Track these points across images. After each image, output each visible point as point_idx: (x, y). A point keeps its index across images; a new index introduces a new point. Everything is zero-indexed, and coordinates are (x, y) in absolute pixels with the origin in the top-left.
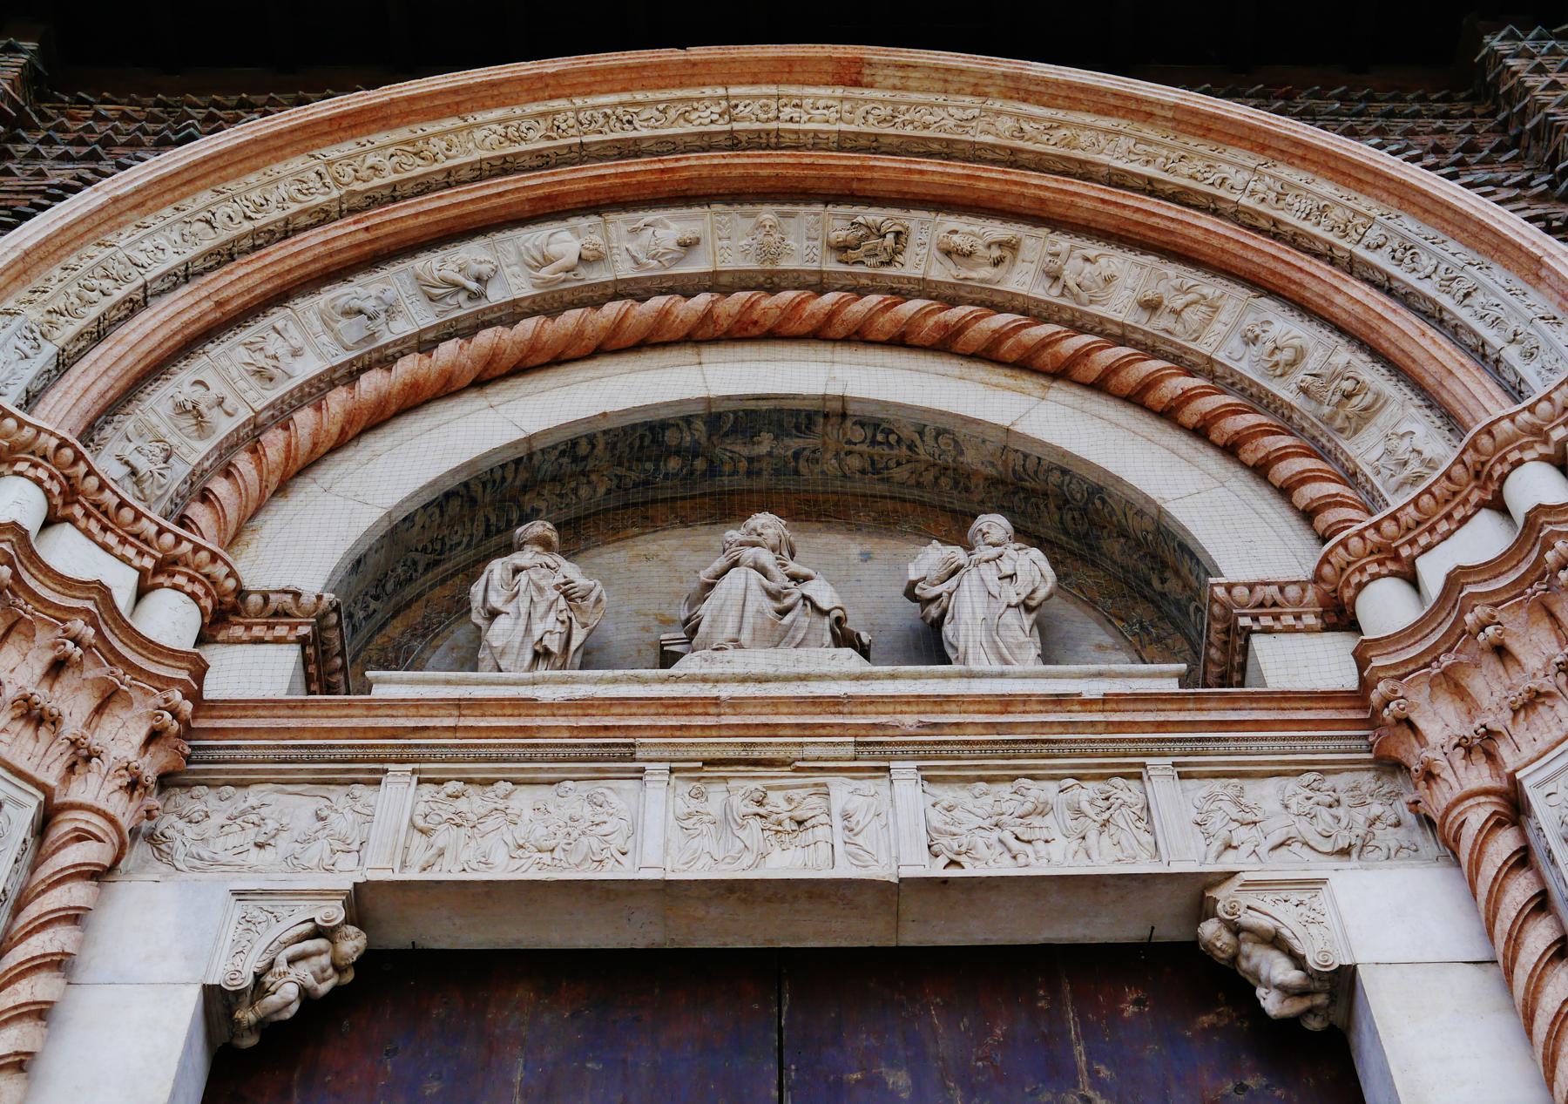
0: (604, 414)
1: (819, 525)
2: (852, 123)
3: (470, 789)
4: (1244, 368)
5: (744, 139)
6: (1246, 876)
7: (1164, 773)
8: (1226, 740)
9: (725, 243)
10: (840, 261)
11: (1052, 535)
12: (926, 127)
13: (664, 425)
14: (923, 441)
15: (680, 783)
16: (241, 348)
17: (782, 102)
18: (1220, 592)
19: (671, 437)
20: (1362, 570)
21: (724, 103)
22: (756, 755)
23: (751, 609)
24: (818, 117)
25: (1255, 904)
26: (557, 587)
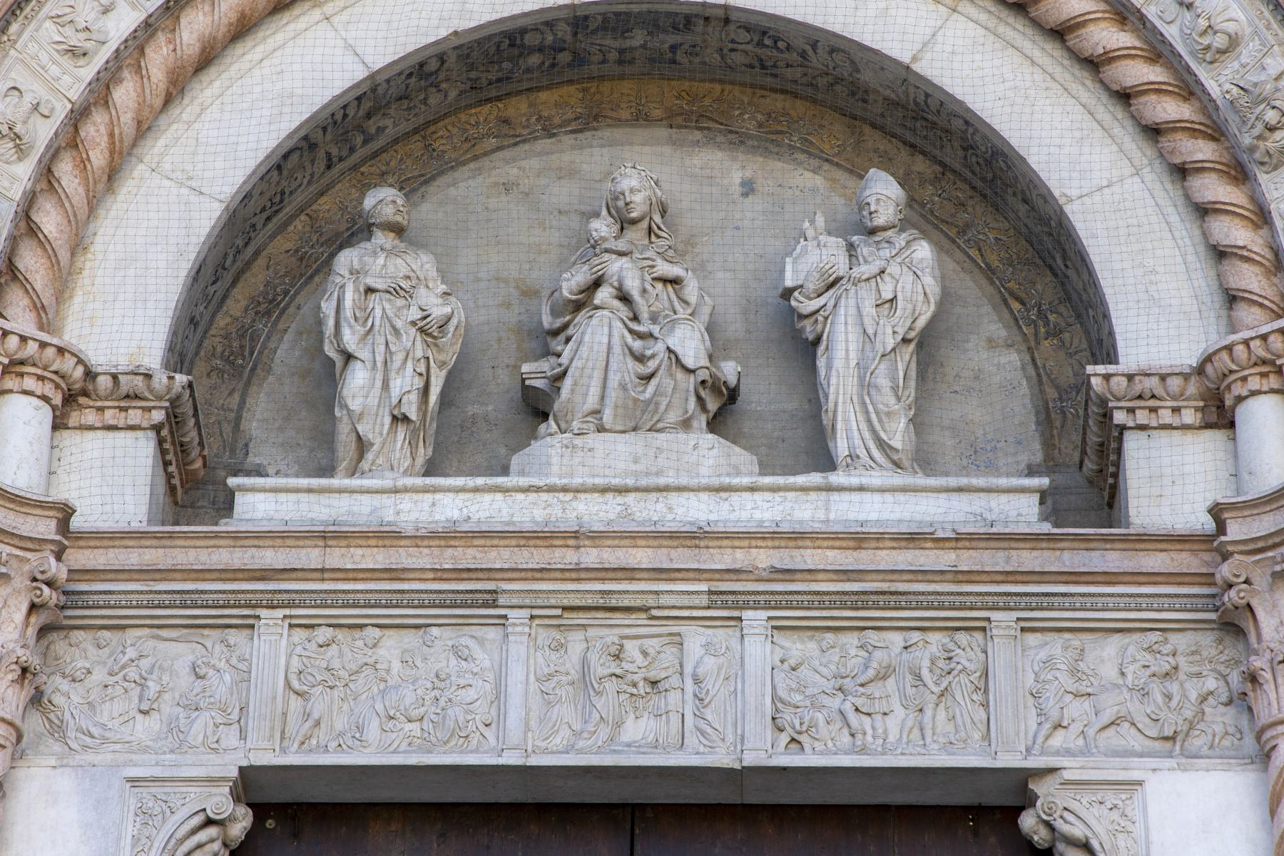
0: (456, 33)
1: (698, 135)
3: (340, 635)
4: (1172, 33)
6: (1067, 775)
7: (1006, 632)
8: (1072, 595)
11: (957, 166)
13: (523, 31)
14: (816, 53)
15: (541, 630)
16: (48, 24)
18: (1095, 381)
19: (530, 40)
22: (614, 603)
23: (614, 380)
25: (1074, 805)
26: (413, 323)
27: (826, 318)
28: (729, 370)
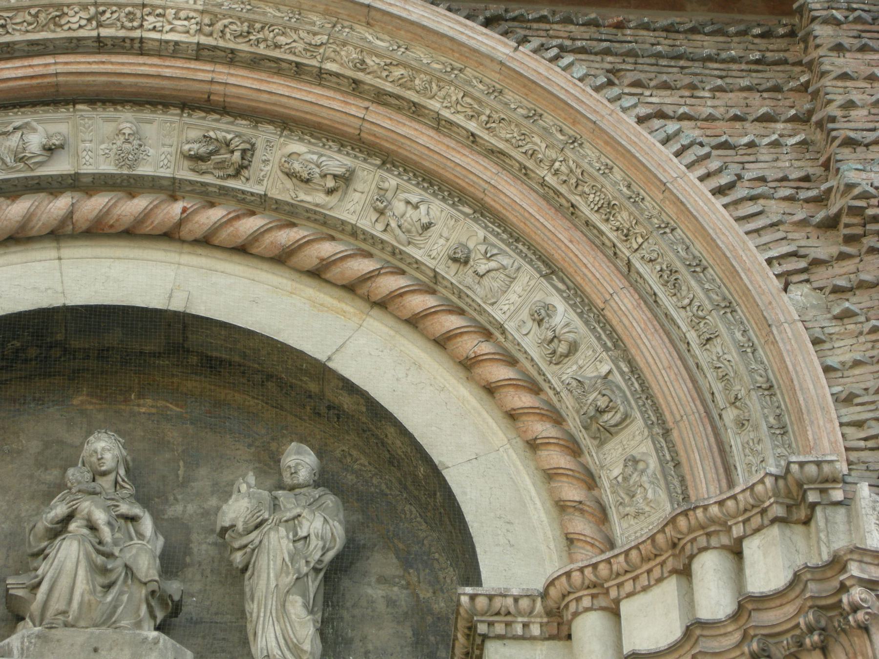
2: (211, 34)
5: (110, 43)
9: (88, 145)
10: (193, 170)
12: (277, 46)
17: (147, 10)
18: (464, 600)
20: (578, 599)
21: (92, 10)
24: (180, 29)
27: (253, 550)
28: (174, 587)
